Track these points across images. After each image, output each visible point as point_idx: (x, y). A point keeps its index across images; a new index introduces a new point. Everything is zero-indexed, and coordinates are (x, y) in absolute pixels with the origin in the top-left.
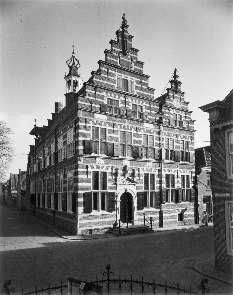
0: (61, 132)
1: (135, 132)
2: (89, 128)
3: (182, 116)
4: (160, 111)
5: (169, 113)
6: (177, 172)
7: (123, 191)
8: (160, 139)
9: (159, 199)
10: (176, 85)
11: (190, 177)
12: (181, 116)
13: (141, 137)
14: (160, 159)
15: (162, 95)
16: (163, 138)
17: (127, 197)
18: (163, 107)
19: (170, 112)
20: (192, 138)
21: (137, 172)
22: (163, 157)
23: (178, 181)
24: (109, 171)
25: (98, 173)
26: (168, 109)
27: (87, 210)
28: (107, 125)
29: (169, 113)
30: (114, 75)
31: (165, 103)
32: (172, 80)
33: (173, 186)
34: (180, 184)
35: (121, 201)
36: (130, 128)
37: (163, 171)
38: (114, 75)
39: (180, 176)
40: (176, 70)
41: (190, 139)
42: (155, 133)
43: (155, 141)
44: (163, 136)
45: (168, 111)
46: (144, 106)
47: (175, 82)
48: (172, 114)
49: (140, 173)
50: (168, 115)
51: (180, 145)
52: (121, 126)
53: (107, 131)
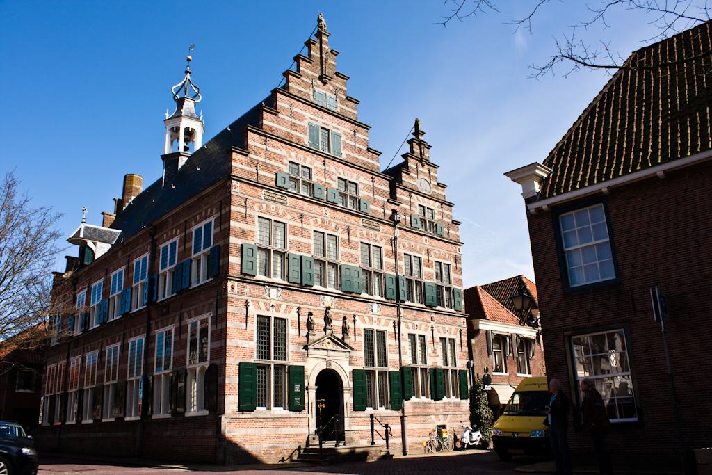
0: (172, 230)
1: (346, 236)
2: (251, 219)
3: (435, 211)
4: (393, 196)
6: (432, 330)
7: (323, 366)
9: (401, 387)
11: (457, 342)
13: (356, 248)
14: (398, 299)
15: (389, 167)
16: (400, 254)
17: (329, 380)
18: (398, 190)
19: (412, 200)
20: (456, 259)
21: (350, 324)
22: (403, 296)
23: (434, 351)
24: (292, 316)
25: (269, 318)
26: (408, 194)
27: (246, 405)
28: (289, 216)
29: (411, 204)
31: (401, 182)
33: (425, 362)
34: (438, 356)
35: (317, 387)
36: (333, 225)
39: (438, 340)
41: (452, 259)
42: (384, 241)
43: (385, 259)
44: (401, 251)
45: (408, 199)
50: (408, 207)
51: (433, 271)
52: (316, 220)
53: (288, 230)
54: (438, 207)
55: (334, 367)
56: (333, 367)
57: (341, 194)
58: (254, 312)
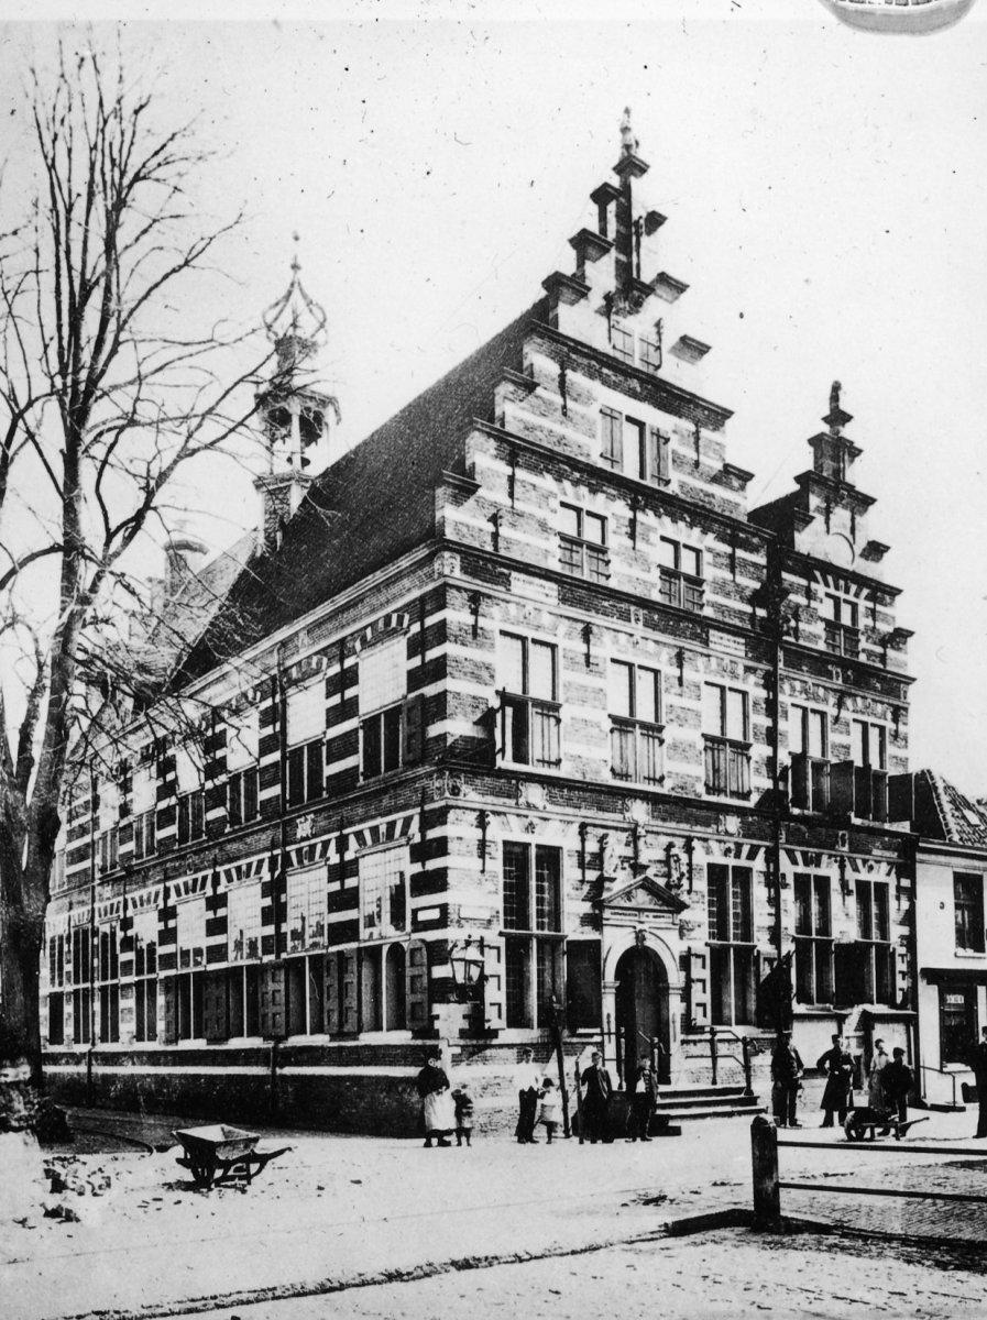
3: (861, 609)
5: (809, 594)
8: (772, 708)
10: (837, 458)
12: (854, 607)
19: (814, 586)
29: (809, 594)
30: (589, 399)
32: (823, 434)
37: (783, 856)
38: (589, 399)
39: (852, 886)
40: (836, 388)
41: (889, 716)
44: (784, 698)
46: (710, 550)
47: (834, 448)
48: (821, 594)
49: (694, 862)
50: (802, 601)
53: (561, 662)
54: (867, 598)
55: (650, 943)
56: (648, 943)
57: (665, 571)
58: (498, 832)
